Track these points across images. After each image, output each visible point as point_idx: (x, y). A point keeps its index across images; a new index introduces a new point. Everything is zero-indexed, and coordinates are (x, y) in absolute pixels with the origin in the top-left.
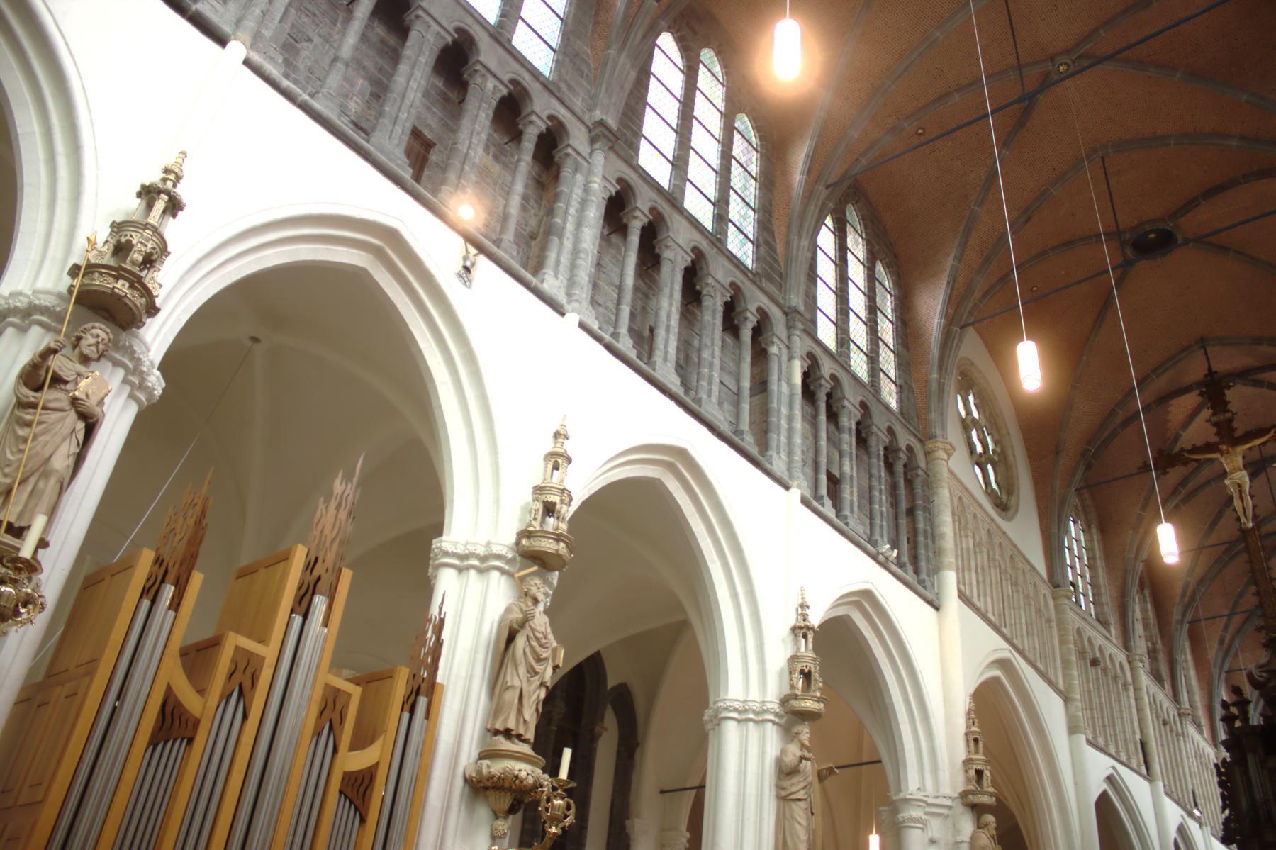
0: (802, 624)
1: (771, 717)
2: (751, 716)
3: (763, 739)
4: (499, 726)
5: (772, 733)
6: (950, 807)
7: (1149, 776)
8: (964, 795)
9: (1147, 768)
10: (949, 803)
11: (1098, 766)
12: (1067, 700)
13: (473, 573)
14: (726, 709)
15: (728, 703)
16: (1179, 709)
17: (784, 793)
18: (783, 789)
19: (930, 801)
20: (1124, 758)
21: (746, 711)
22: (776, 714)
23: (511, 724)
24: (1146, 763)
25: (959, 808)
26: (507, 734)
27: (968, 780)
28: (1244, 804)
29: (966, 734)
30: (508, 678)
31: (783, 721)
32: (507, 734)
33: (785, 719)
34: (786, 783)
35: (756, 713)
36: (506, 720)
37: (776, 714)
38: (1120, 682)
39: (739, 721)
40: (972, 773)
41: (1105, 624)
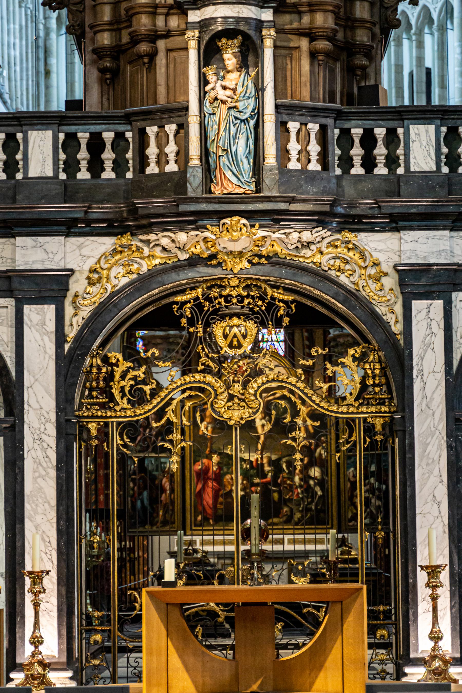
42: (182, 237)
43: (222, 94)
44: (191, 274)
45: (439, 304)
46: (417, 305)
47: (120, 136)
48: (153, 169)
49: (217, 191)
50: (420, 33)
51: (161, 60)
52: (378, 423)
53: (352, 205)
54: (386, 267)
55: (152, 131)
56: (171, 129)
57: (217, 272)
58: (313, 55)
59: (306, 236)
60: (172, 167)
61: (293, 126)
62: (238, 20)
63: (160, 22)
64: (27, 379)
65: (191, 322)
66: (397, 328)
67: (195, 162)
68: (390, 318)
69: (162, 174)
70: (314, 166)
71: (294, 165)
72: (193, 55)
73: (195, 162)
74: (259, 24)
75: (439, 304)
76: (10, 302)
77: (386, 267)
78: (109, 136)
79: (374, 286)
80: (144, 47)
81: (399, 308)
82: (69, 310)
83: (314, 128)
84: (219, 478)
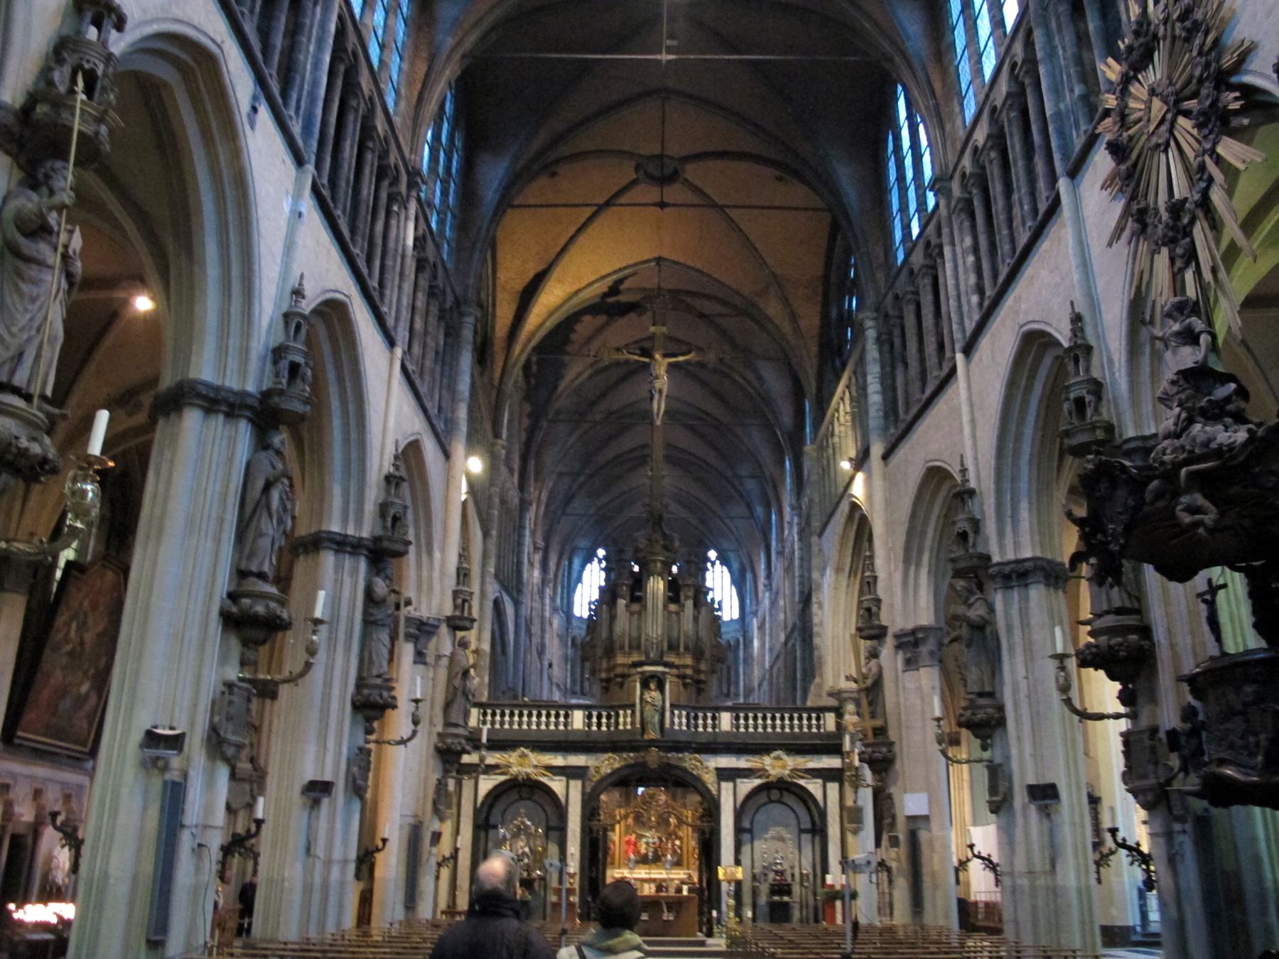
0: (397, 474)
3: (355, 571)
4: (254, 568)
11: (493, 589)
12: (486, 534)
13: (221, 417)
16: (535, 543)
17: (372, 619)
18: (372, 615)
23: (266, 568)
26: (261, 576)
27: (456, 607)
28: (604, 634)
29: (458, 569)
30: (263, 526)
32: (261, 576)
34: (371, 610)
36: (262, 563)
40: (459, 601)
41: (511, 471)
45: (731, 785)
46: (724, 785)
48: (621, 727)
49: (646, 737)
51: (626, 686)
52: (707, 830)
55: (621, 712)
56: (629, 712)
58: (685, 685)
60: (629, 727)
61: (676, 712)
63: (626, 671)
64: (570, 809)
66: (714, 792)
69: (626, 731)
70: (684, 728)
72: (638, 685)
73: (638, 726)
74: (664, 673)
76: (564, 778)
78: (604, 713)
80: (619, 680)
82: (587, 783)
83: (684, 713)
84: (635, 845)
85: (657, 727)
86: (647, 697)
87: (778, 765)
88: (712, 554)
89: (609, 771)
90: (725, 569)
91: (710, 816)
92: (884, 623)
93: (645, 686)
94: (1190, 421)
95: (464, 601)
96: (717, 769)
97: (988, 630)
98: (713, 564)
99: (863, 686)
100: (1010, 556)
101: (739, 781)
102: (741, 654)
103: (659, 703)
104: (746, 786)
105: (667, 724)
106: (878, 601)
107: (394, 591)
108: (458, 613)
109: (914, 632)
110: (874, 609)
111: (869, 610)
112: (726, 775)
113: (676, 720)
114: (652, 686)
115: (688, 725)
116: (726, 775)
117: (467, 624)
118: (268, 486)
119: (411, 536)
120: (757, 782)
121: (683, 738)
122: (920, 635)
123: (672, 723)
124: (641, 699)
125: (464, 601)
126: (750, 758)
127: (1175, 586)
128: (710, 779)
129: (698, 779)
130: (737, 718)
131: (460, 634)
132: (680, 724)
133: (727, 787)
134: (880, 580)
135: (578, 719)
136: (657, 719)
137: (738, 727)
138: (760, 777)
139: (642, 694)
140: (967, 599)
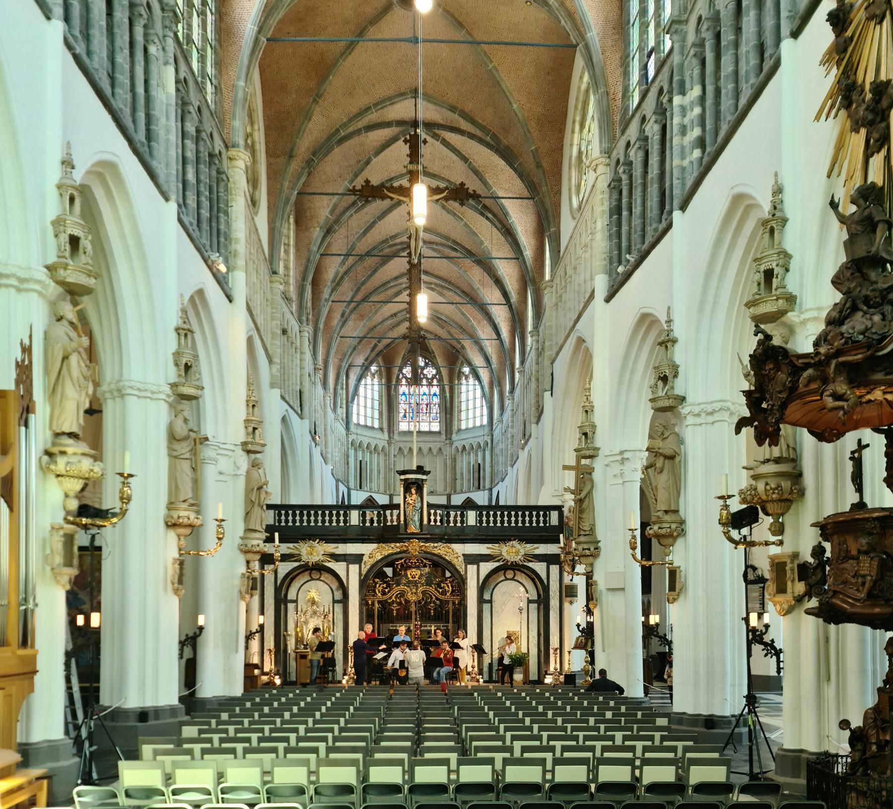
1: (164, 397)
2: (149, 395)
5: (164, 408)
6: (233, 451)
7: (301, 417)
8: (244, 444)
9: (301, 410)
10: (233, 448)
14: (131, 387)
15: (133, 384)
19: (222, 446)
20: (292, 403)
21: (146, 390)
22: (168, 396)
24: (301, 406)
25: (239, 452)
27: (248, 434)
29: (247, 401)
31: (171, 400)
33: (172, 398)
35: (153, 393)
37: (168, 396)
38: (294, 346)
39: (139, 397)
40: (251, 429)
42: (398, 545)
43: (411, 502)
44: (400, 556)
45: (475, 566)
46: (469, 566)
47: (379, 512)
48: (389, 524)
49: (409, 531)
50: (477, 451)
53: (450, 535)
54: (460, 554)
57: (408, 555)
59: (436, 545)
60: (395, 523)
62: (416, 479)
65: (400, 570)
66: (463, 573)
67: (402, 522)
68: (460, 570)
69: (392, 525)
70: (439, 523)
71: (432, 523)
73: (402, 522)
75: (475, 566)
77: (460, 554)
79: (456, 560)
81: (463, 567)
85: (418, 524)
86: (409, 499)
87: (513, 551)
88: (466, 370)
89: (380, 557)
90: (477, 383)
91: (459, 591)
92: (598, 445)
93: (407, 490)
94: (854, 309)
95: (254, 429)
96: (464, 555)
97: (677, 459)
98: (467, 377)
99: (578, 497)
100: (700, 399)
101: (481, 564)
102: (488, 453)
103: (418, 505)
104: (486, 567)
105: (425, 521)
106: (594, 427)
107: (191, 430)
108: (250, 440)
109: (622, 453)
110: (590, 435)
111: (585, 434)
112: (472, 559)
113: (432, 518)
114: (413, 491)
115: (441, 521)
116: (472, 559)
117: (258, 448)
118: (65, 358)
119: (206, 383)
120: (497, 564)
121: (437, 531)
122: (626, 455)
123: (429, 521)
124: (405, 502)
125: (254, 429)
126: (490, 545)
127: (827, 447)
128: (459, 564)
129: (449, 563)
130: (481, 515)
131: (253, 456)
132: (435, 521)
133: (472, 569)
134: (595, 410)
135: (354, 518)
136: (416, 518)
137: (481, 522)
138: (498, 561)
139: (405, 498)
140: (663, 434)
